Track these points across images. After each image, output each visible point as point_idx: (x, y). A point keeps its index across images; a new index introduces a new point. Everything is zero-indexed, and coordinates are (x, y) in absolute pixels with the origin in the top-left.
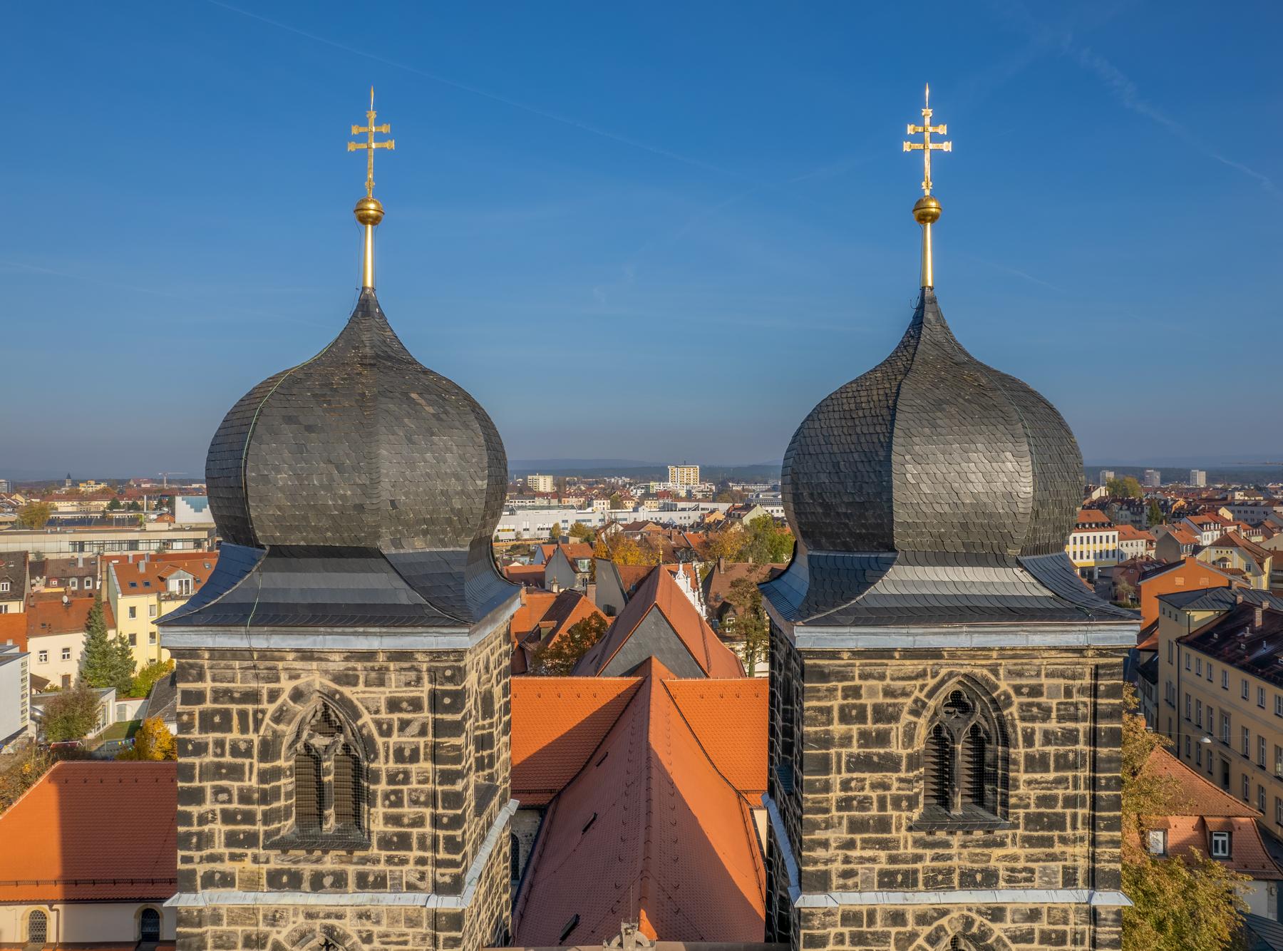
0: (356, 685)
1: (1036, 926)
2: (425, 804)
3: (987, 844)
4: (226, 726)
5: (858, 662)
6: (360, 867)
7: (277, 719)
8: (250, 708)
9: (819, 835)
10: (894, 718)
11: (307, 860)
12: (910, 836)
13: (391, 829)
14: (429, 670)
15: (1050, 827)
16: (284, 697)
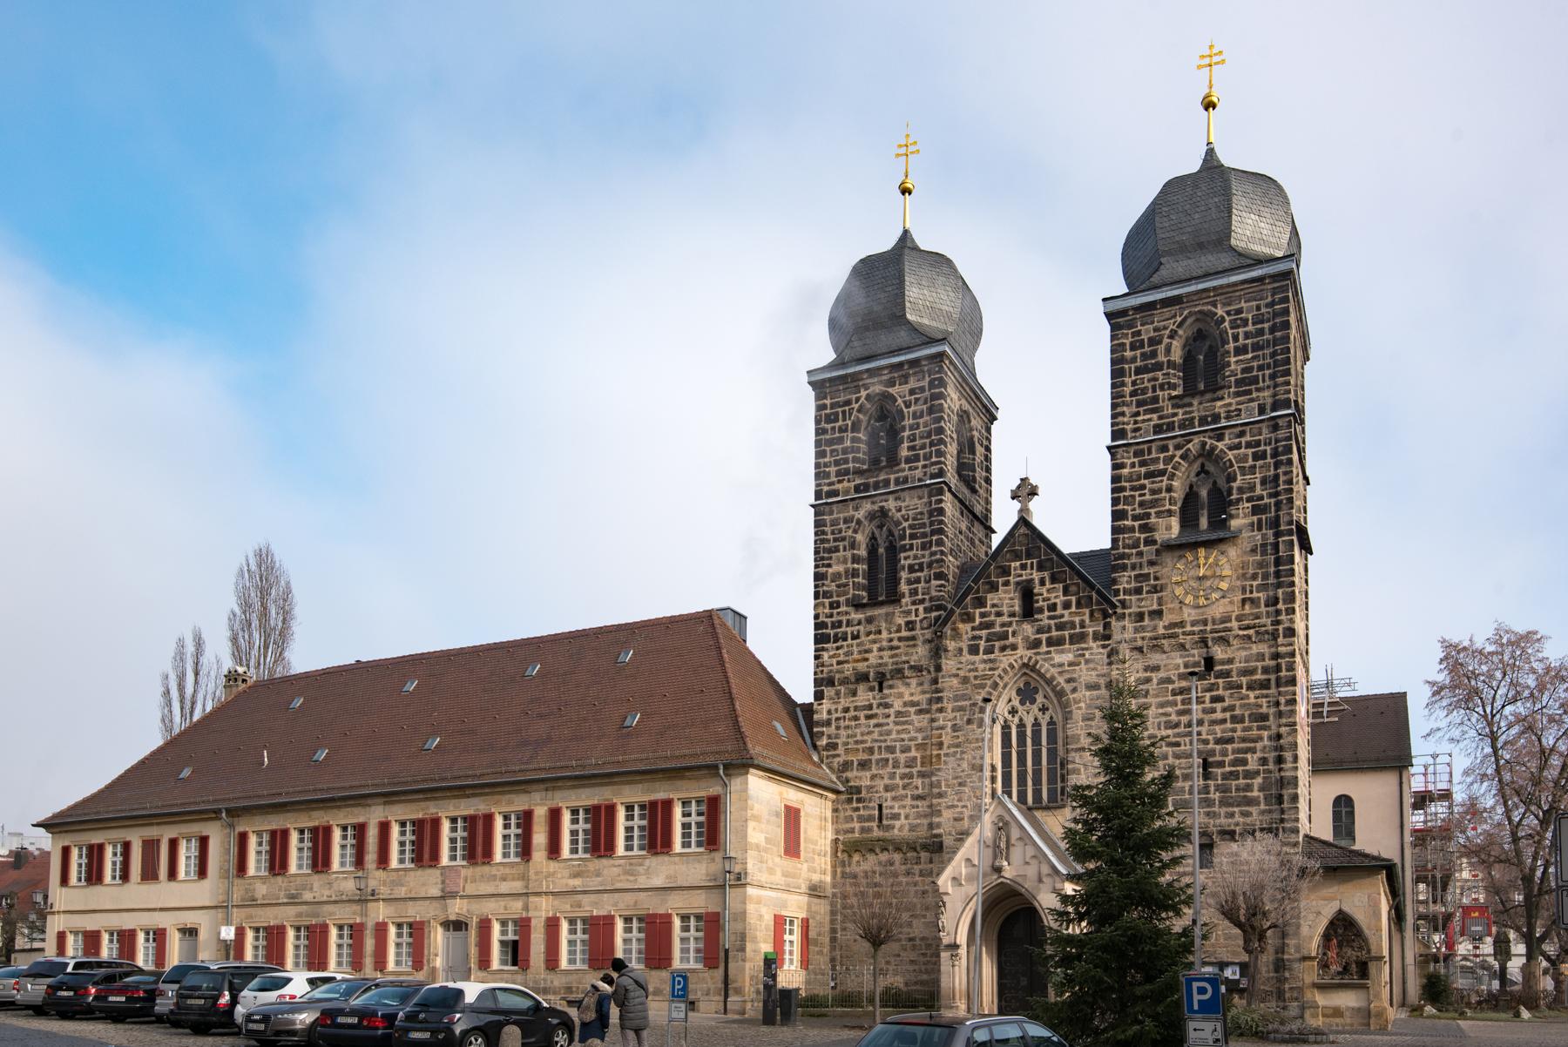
1: (1243, 440)
3: (1214, 400)
4: (836, 420)
7: (859, 411)
9: (1119, 410)
10: (1160, 342)
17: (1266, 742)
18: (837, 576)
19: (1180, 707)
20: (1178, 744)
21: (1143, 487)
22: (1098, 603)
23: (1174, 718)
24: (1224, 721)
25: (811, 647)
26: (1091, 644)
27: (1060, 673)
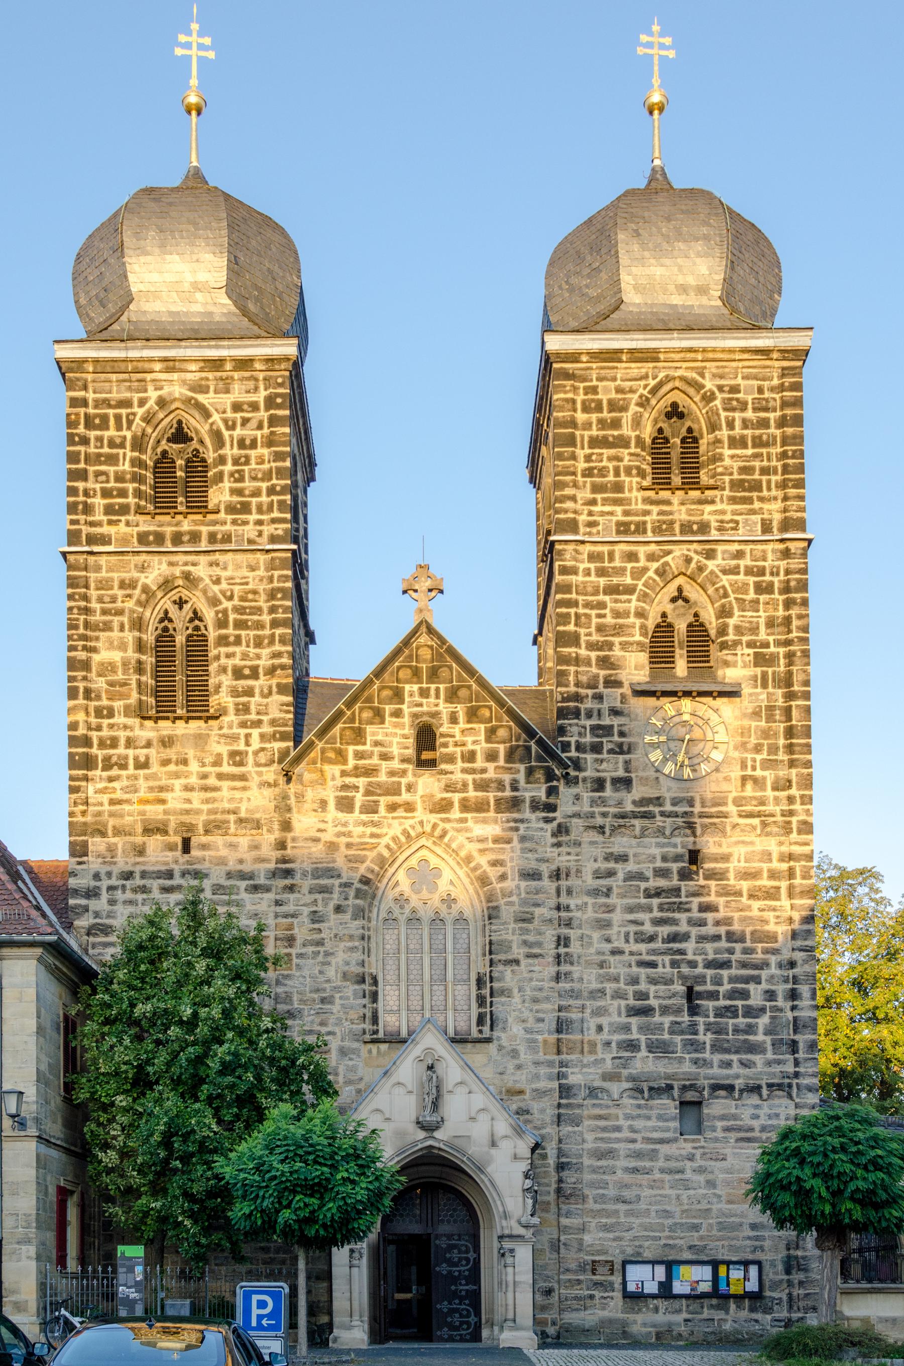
0: (207, 392)
2: (263, 480)
4: (104, 425)
5: (594, 366)
6: (211, 528)
8: (124, 412)
11: (169, 524)
12: (640, 495)
13: (236, 499)
14: (265, 379)
15: (751, 489)
16: (151, 403)
17: (774, 970)
18: (108, 668)
19: (657, 914)
20: (653, 965)
21: (602, 605)
22: (540, 759)
23: (648, 928)
24: (717, 938)
25: (64, 772)
26: (527, 814)
27: (482, 851)
